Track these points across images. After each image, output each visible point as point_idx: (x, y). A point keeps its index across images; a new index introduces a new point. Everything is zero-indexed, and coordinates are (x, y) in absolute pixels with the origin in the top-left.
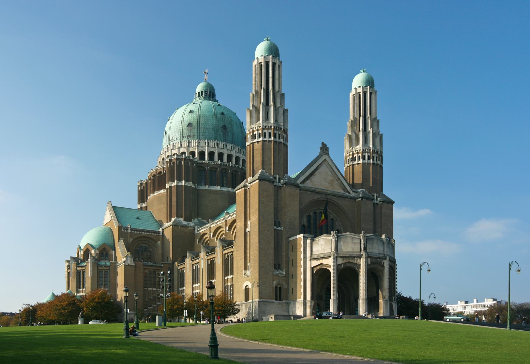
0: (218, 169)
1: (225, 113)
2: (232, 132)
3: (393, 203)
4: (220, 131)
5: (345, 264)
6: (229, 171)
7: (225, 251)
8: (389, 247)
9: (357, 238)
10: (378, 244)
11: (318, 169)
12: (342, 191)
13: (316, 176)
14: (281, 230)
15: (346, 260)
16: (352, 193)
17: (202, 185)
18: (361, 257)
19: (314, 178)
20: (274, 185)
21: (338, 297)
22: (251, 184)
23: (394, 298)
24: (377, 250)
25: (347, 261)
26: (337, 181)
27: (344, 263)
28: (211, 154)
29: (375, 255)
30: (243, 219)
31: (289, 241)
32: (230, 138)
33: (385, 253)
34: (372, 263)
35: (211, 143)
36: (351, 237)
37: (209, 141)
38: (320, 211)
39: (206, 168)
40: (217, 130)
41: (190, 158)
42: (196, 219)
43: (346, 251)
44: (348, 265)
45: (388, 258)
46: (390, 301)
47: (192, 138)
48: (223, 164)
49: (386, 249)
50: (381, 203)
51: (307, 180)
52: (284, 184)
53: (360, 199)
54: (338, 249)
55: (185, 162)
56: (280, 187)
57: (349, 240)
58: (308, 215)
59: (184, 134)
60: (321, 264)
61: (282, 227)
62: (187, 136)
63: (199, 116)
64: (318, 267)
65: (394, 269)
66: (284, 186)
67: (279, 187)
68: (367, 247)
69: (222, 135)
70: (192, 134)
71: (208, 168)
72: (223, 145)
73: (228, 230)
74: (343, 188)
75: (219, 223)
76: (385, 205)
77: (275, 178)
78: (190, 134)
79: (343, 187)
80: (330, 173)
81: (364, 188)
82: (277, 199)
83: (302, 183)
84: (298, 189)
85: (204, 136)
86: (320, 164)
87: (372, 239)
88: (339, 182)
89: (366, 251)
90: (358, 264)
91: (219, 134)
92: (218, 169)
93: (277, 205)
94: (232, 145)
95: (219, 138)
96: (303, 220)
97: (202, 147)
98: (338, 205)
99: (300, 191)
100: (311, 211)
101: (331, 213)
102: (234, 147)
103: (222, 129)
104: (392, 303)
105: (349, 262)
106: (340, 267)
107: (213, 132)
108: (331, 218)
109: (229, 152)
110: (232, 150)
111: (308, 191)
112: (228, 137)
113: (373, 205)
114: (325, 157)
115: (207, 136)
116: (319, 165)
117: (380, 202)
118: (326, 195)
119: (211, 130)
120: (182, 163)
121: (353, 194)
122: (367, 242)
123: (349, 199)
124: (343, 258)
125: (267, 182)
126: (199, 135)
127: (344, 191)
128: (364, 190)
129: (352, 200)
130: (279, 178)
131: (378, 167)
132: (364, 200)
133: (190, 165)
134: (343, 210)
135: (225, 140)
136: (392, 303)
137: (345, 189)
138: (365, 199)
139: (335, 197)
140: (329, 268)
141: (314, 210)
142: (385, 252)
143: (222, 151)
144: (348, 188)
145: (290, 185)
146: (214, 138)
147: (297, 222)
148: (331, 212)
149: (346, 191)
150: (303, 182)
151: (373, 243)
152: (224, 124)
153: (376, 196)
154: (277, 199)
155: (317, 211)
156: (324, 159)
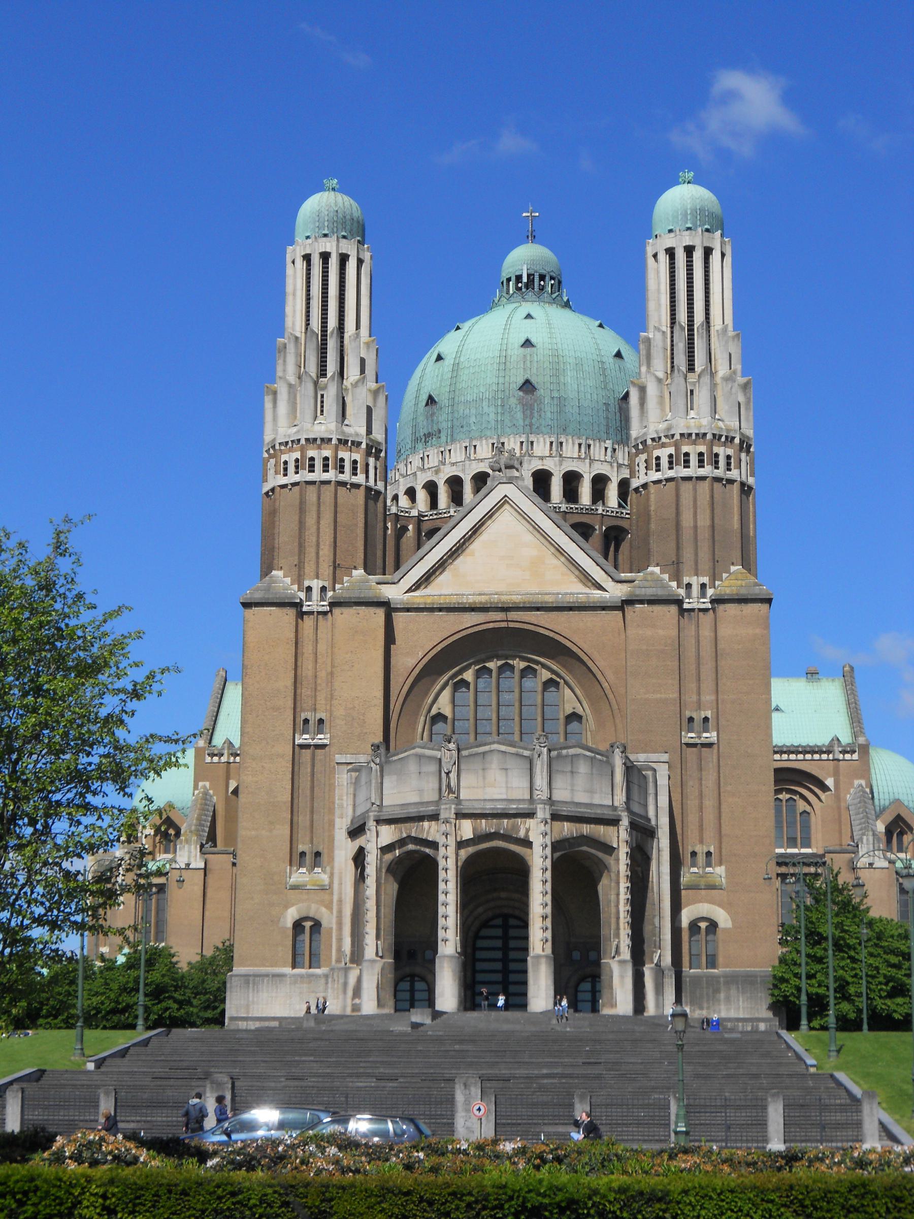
1: (533, 340)
2: (556, 394)
4: (513, 401)
23: (616, 943)
24: (504, 790)
25: (404, 835)
29: (489, 807)
32: (549, 415)
35: (482, 445)
37: (477, 443)
38: (500, 663)
40: (502, 399)
51: (441, 573)
52: (332, 605)
56: (325, 613)
57: (412, 767)
61: (328, 736)
63: (456, 367)
70: (435, 428)
74: (577, 577)
76: (731, 609)
78: (432, 426)
79: (577, 573)
81: (657, 565)
85: (465, 429)
95: (509, 425)
97: (453, 464)
98: (551, 635)
103: (521, 393)
104: (610, 961)
106: (389, 857)
107: (492, 409)
118: (505, 609)
119: (485, 404)
122: (463, 767)
124: (393, 826)
128: (657, 570)
138: (641, 602)
144: (597, 574)
151: (483, 769)
152: (527, 376)
153: (703, 586)
155: (491, 665)
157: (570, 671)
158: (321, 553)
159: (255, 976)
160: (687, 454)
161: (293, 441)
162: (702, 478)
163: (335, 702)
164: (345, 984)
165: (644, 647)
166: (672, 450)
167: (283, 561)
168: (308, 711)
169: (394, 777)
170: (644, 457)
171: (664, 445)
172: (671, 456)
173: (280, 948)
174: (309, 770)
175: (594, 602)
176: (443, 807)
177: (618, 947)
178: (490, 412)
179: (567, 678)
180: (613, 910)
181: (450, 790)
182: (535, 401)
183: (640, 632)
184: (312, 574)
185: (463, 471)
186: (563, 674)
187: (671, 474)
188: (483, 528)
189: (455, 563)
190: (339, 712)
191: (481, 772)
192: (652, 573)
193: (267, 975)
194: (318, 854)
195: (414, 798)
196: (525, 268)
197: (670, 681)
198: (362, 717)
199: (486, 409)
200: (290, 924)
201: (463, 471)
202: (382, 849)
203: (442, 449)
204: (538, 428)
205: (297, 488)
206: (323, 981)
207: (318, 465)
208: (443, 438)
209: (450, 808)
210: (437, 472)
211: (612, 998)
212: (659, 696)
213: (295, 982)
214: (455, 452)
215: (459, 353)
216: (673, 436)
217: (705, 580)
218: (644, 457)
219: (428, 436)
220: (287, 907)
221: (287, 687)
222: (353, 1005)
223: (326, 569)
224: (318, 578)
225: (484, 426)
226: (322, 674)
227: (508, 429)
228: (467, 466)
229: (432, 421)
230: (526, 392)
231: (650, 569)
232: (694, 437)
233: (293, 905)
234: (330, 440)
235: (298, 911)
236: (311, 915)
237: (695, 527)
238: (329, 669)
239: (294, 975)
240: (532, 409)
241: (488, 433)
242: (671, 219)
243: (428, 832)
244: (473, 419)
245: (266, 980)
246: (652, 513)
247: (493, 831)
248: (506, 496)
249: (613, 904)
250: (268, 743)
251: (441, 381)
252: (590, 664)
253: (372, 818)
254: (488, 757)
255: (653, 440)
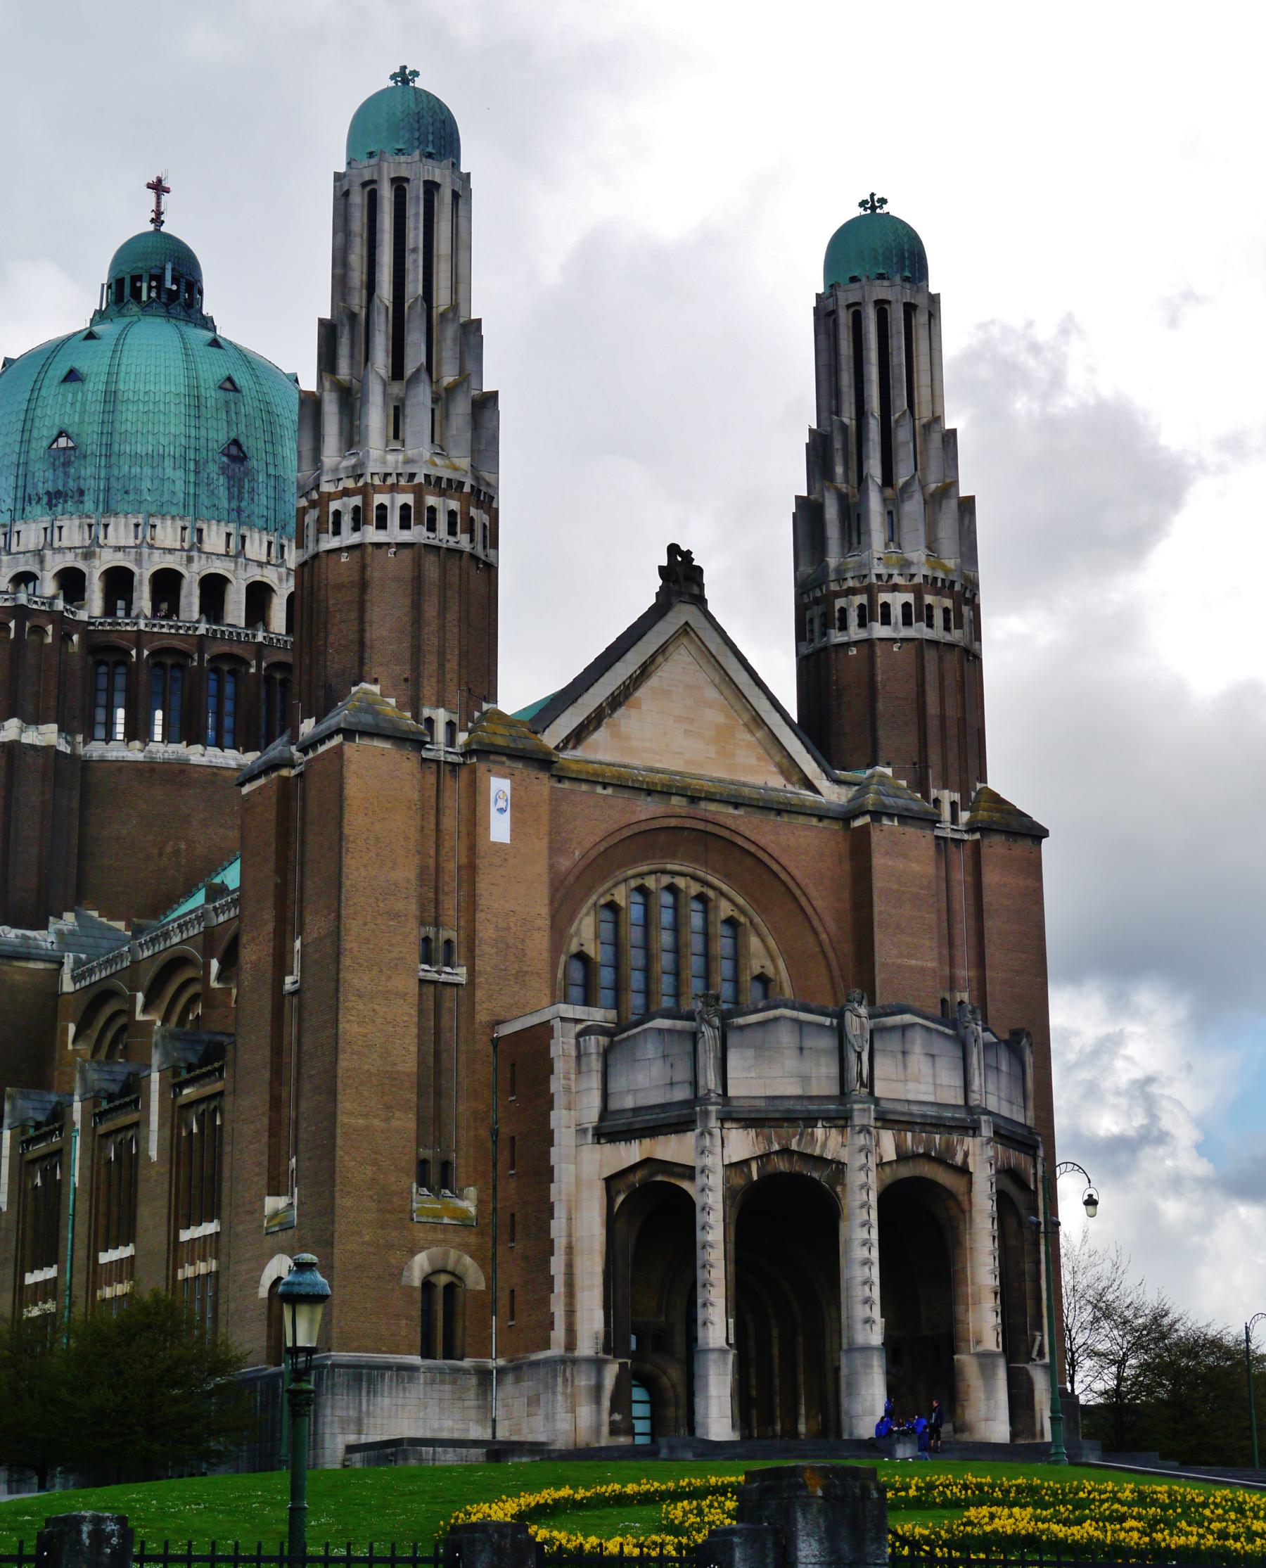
0: (196, 657)
2: (271, 471)
3: (1037, 834)
4: (213, 469)
5: (764, 1158)
6: (250, 665)
7: (186, 1091)
8: (998, 1069)
9: (822, 1026)
10: (933, 1056)
11: (649, 676)
12: (777, 781)
13: (640, 708)
14: (457, 985)
15: (770, 1142)
16: (821, 790)
17: (112, 740)
18: (845, 1127)
19: (625, 718)
20: (424, 760)
21: (732, 1341)
22: (311, 755)
24: (931, 1088)
25: (776, 1147)
26: (751, 732)
27: (760, 1157)
28: (167, 584)
30: (270, 927)
31: (496, 1042)
32: (263, 498)
33: (972, 1103)
34: (903, 1156)
35: (164, 528)
36: (796, 1021)
37: (158, 522)
38: (666, 880)
39: (134, 653)
41: (51, 605)
42: (69, 917)
43: (768, 1094)
44: (782, 1165)
45: (987, 1131)
46: (1008, 1362)
47: (70, 503)
48: (223, 632)
49: (976, 1083)
50: (977, 836)
51: (596, 729)
52: (468, 752)
53: (867, 819)
54: (729, 1082)
55: (28, 624)
56: (453, 764)
57: (786, 1037)
58: (602, 901)
59: (35, 486)
60: (647, 1162)
62: (48, 493)
64: (636, 1178)
65: (1032, 1187)
66: (474, 760)
67: (448, 768)
68: (877, 1073)
69: (222, 489)
71: (146, 653)
72: (228, 535)
73: (219, 978)
74: (778, 765)
75: (176, 940)
76: (995, 848)
77: (430, 722)
79: (778, 758)
80: (712, 694)
81: (888, 764)
82: (438, 823)
83: (570, 746)
84: (544, 776)
85: (132, 496)
86: (662, 650)
87: (905, 1028)
88: (759, 734)
89: (871, 1093)
90: (832, 1161)
91: (208, 485)
92: (196, 657)
93: (437, 854)
94: (272, 539)
96: (578, 931)
98: (752, 849)
99: (560, 786)
100: (616, 885)
101: (722, 894)
102: (282, 547)
103: (225, 459)
104: (1029, 1367)
105: (785, 1151)
106: (739, 1181)
108: (723, 916)
109: (256, 574)
110: (268, 563)
111: (598, 783)
112: (253, 499)
113: (938, 845)
114: (682, 614)
115: (145, 492)
116: (653, 658)
117: (971, 829)
119: (168, 463)
120: (10, 628)
121: (832, 794)
122: (876, 1046)
123: (814, 821)
124: (752, 1132)
125: (387, 745)
126: (108, 490)
127: (788, 778)
128: (889, 771)
129: (825, 823)
130: (450, 725)
131: (952, 659)
132: (885, 821)
133: (49, 640)
134: (783, 876)
135: (238, 515)
136: (1029, 1367)
137: (790, 768)
138: (891, 816)
139: (736, 812)
140: (685, 1185)
141: (634, 877)
142: (975, 1099)
143: (219, 567)
144: (809, 766)
145: (504, 759)
146: (182, 506)
147: (539, 943)
148: (724, 887)
149: (795, 779)
150: (578, 736)
151: (904, 1053)
152: (233, 435)
153: (953, 804)
154: (438, 823)
155: (650, 882)
156: (682, 622)
157: (762, 911)
158: (448, 666)
159: (372, 1367)
160: (930, 607)
161: (399, 475)
162: (951, 646)
163: (480, 915)
164: (598, 1388)
165: (896, 887)
166: (909, 598)
167: (379, 669)
168: (430, 925)
169: (750, 1053)
170: (861, 599)
171: (895, 588)
172: (906, 606)
173: (404, 1322)
174: (432, 1023)
175: (811, 808)
176: (856, 1106)
177: (1041, 1346)
178: (177, 479)
179: (757, 920)
180: (1029, 1286)
181: (862, 1085)
182: (246, 474)
183: (890, 863)
184: (434, 699)
185: (139, 562)
186: (751, 912)
187: (905, 633)
188: (653, 667)
189: (615, 715)
190: (486, 931)
191: (900, 1056)
192: (884, 776)
193: (388, 1367)
194: (446, 1166)
195: (792, 1089)
196: (169, 267)
197: (927, 943)
198: (520, 946)
199: (169, 472)
200: (417, 1282)
201: (139, 562)
202: (731, 1165)
203: (93, 521)
204: (248, 516)
205: (406, 554)
206: (473, 1381)
207: (394, 519)
208: (89, 505)
209: (869, 1109)
210: (88, 555)
211: (1034, 1424)
212: (913, 962)
213: (433, 1382)
214: (116, 530)
215: (112, 375)
216: (913, 576)
217: (956, 797)
218: (861, 599)
219: (54, 498)
220: (413, 1253)
221: (408, 881)
222: (612, 1423)
223: (455, 697)
224: (443, 706)
225: (166, 498)
226: (451, 867)
227: (205, 510)
228: (145, 556)
229: (66, 474)
230: (233, 459)
231: (879, 769)
232: (939, 584)
233: (423, 1249)
234: (461, 484)
235: (430, 1260)
236: (449, 1268)
237: (942, 718)
238: (464, 861)
239: (429, 1369)
240: (241, 487)
241: (174, 511)
242: (880, 259)
243: (824, 1145)
244: (146, 484)
245: (388, 1374)
246: (879, 686)
247: (921, 1151)
248: (687, 623)
249: (1027, 1278)
250: (381, 971)
251: (83, 412)
252: (803, 900)
253: (713, 1116)
254: (909, 1033)
255: (879, 576)
